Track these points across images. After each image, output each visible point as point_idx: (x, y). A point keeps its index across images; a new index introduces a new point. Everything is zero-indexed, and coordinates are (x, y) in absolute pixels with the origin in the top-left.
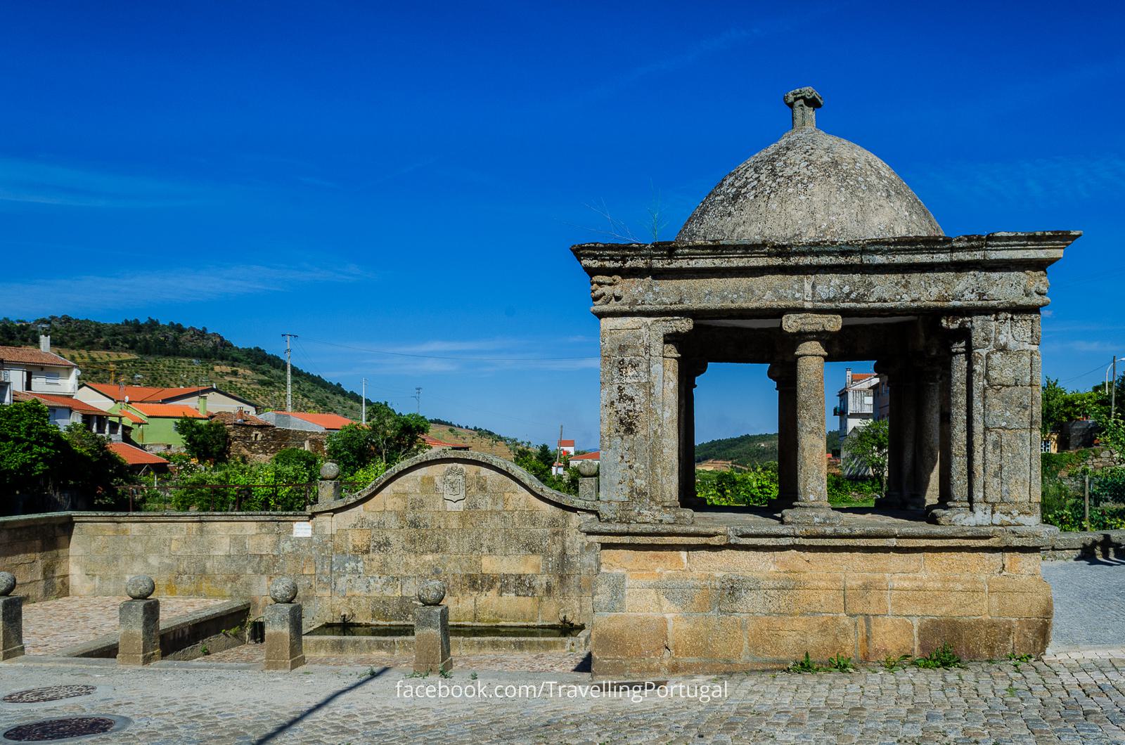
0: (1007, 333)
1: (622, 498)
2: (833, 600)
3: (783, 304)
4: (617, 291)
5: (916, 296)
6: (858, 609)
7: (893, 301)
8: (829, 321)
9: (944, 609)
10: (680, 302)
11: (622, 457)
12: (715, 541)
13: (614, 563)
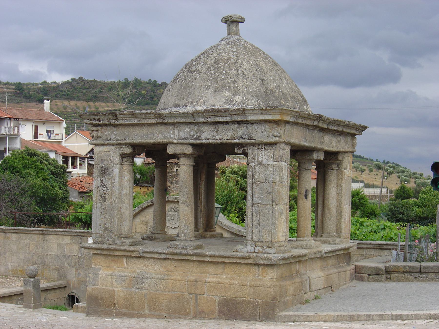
0: (262, 155)
1: (101, 232)
2: (183, 286)
3: (168, 141)
4: (99, 134)
5: (221, 137)
6: (193, 291)
7: (212, 139)
8: (186, 149)
9: (229, 293)
10: (125, 139)
11: (101, 213)
12: (134, 255)
13: (97, 263)
